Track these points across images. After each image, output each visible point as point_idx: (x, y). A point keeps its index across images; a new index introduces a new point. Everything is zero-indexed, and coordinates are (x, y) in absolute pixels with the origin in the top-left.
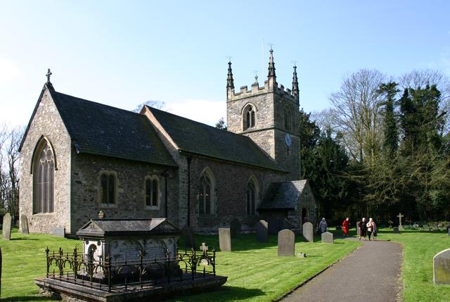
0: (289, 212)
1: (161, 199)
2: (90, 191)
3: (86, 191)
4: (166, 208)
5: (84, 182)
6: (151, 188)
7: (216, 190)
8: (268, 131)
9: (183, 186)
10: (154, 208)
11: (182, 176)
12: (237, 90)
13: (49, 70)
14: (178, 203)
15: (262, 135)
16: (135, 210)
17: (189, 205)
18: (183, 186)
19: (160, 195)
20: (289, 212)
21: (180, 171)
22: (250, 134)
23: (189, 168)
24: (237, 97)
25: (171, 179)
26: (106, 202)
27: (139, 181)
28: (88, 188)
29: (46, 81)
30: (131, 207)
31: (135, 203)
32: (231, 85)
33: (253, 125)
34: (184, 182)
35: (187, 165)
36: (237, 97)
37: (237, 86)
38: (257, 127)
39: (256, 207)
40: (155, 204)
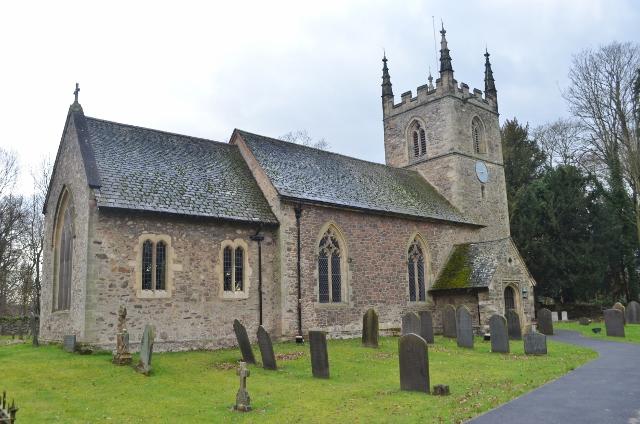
0: (480, 296)
1: (252, 280)
2: (122, 270)
3: (113, 270)
4: (261, 293)
5: (112, 256)
6: (233, 261)
7: (350, 260)
8: (446, 159)
9: (287, 258)
11: (285, 236)
12: (397, 100)
13: (77, 85)
14: (280, 284)
15: (437, 166)
16: (203, 300)
17: (299, 286)
18: (287, 258)
19: (249, 272)
20: (480, 296)
21: (282, 229)
22: (418, 167)
23: (298, 224)
24: (397, 111)
25: (269, 244)
26: (150, 288)
27: (211, 249)
28: (117, 265)
29: (72, 101)
30: (195, 295)
31: (203, 288)
32: (387, 92)
33: (424, 151)
34: (289, 250)
35: (295, 220)
36: (397, 111)
37: (398, 93)
38: (430, 154)
39: (427, 289)
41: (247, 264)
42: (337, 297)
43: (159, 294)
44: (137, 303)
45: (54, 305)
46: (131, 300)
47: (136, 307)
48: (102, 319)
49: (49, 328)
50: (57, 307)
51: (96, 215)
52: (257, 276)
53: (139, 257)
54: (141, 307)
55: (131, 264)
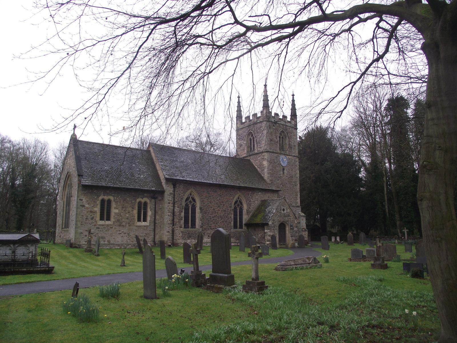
2: (91, 212)
3: (87, 212)
4: (155, 223)
5: (87, 206)
10: (144, 224)
11: (168, 197)
17: (173, 220)
19: (149, 213)
21: (166, 194)
23: (174, 191)
26: (103, 220)
28: (89, 210)
30: (124, 224)
31: (127, 220)
35: (173, 189)
40: (145, 220)
41: (149, 210)
42: (193, 225)
43: (108, 223)
44: (97, 226)
45: (62, 226)
46: (95, 225)
47: (97, 228)
48: (82, 233)
49: (60, 236)
50: (64, 227)
51: (81, 188)
52: (153, 216)
53: (99, 206)
54: (99, 228)
55: (96, 209)
